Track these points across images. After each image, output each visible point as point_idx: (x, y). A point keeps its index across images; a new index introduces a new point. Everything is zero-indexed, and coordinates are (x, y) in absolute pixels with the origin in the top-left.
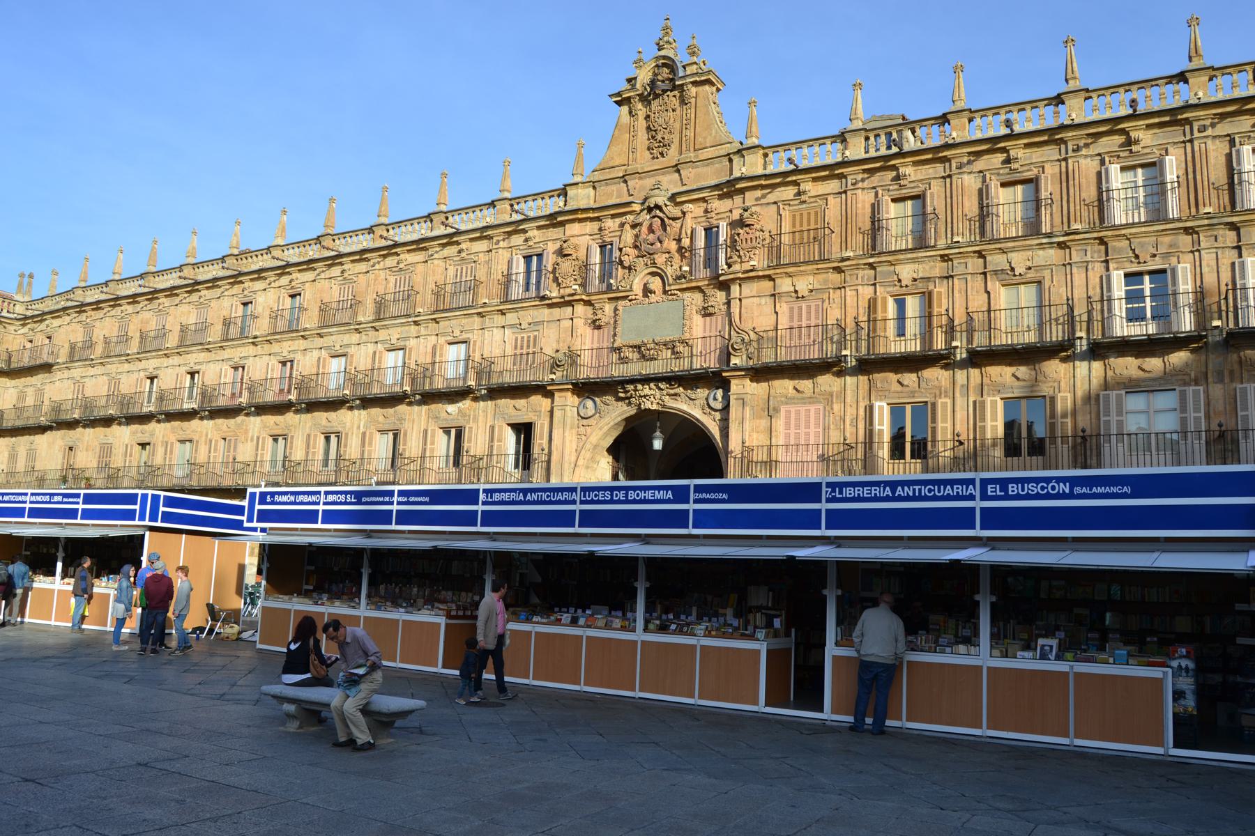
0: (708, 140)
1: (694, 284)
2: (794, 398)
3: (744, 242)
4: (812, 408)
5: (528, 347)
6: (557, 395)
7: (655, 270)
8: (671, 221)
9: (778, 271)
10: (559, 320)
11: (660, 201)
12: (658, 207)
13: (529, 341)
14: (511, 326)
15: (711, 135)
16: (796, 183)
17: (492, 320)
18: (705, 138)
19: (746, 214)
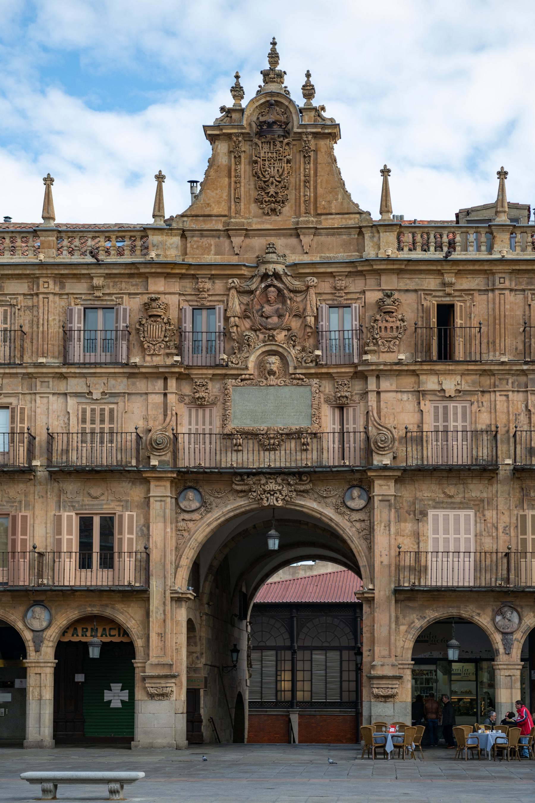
0: (333, 206)
1: (324, 370)
2: (443, 502)
3: (383, 329)
4: (462, 513)
5: (102, 421)
6: (153, 484)
7: (274, 348)
8: (292, 295)
9: (425, 367)
10: (146, 394)
11: (280, 268)
12: (276, 276)
13: (102, 415)
14: (76, 395)
15: (337, 200)
16: (440, 273)
17: (45, 384)
18: (329, 202)
19: (389, 301)
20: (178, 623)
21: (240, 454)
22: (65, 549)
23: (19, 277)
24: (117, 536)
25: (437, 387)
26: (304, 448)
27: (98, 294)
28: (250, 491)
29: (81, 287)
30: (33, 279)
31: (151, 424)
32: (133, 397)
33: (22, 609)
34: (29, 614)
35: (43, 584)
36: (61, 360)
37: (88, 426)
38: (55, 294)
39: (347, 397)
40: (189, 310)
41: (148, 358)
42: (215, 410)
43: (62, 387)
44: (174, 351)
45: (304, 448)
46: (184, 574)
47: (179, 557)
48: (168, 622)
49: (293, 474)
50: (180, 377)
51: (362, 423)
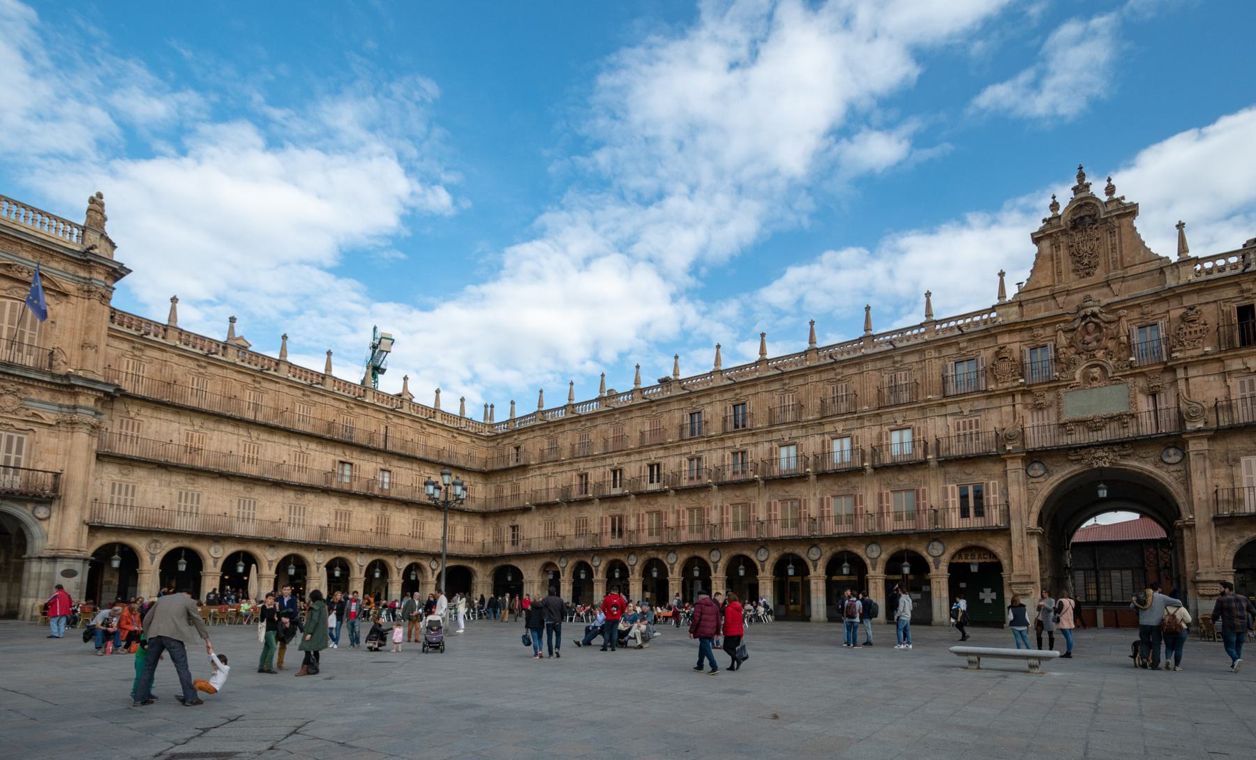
5: (971, 428)
6: (1008, 462)
9: (1229, 354)
14: (952, 414)
20: (1032, 549)
21: (1073, 436)
22: (951, 506)
23: (912, 352)
24: (985, 496)
25: (1242, 367)
26: (1124, 426)
27: (963, 352)
28: (1082, 459)
29: (952, 351)
30: (922, 352)
31: (1004, 425)
32: (991, 411)
33: (925, 544)
34: (930, 547)
35: (938, 528)
36: (942, 395)
37: (962, 432)
38: (935, 358)
39: (1159, 386)
40: (1027, 350)
41: (1000, 385)
42: (1051, 410)
43: (943, 411)
44: (1018, 377)
45: (1124, 426)
46: (1034, 518)
47: (1030, 507)
48: (1026, 548)
49: (1117, 444)
50: (1024, 393)
51: (1173, 402)
